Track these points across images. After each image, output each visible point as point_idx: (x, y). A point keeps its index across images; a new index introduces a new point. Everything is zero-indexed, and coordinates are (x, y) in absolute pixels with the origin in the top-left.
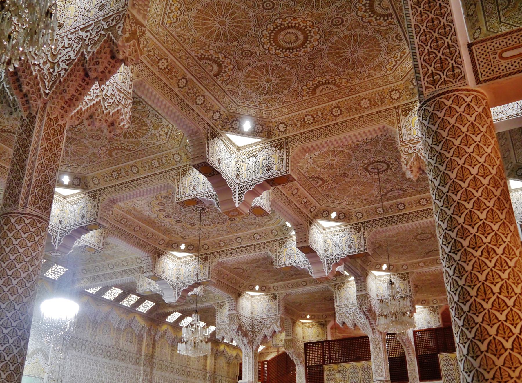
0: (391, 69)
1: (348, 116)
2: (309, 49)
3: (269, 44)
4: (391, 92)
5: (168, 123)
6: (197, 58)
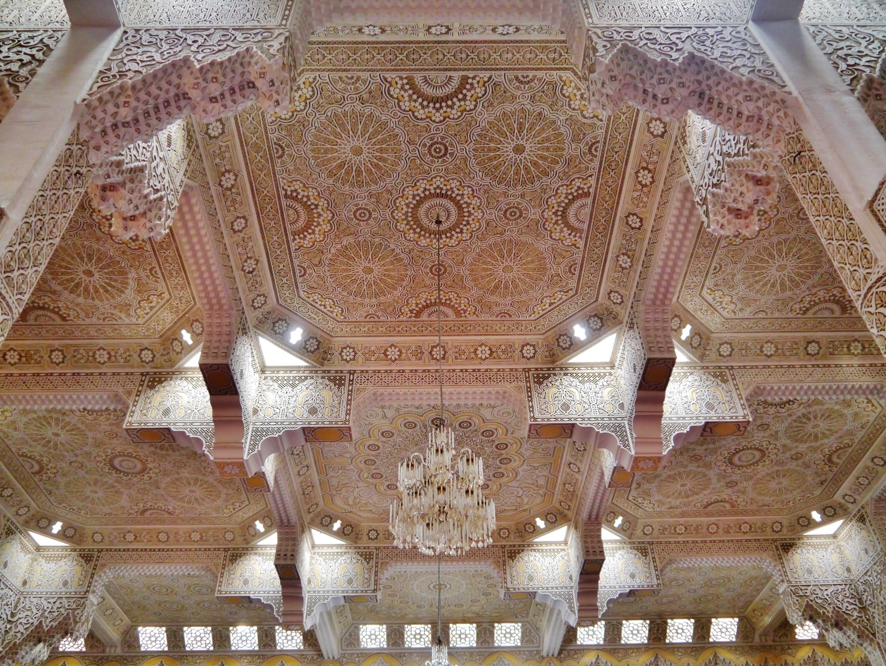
6: (284, 192)
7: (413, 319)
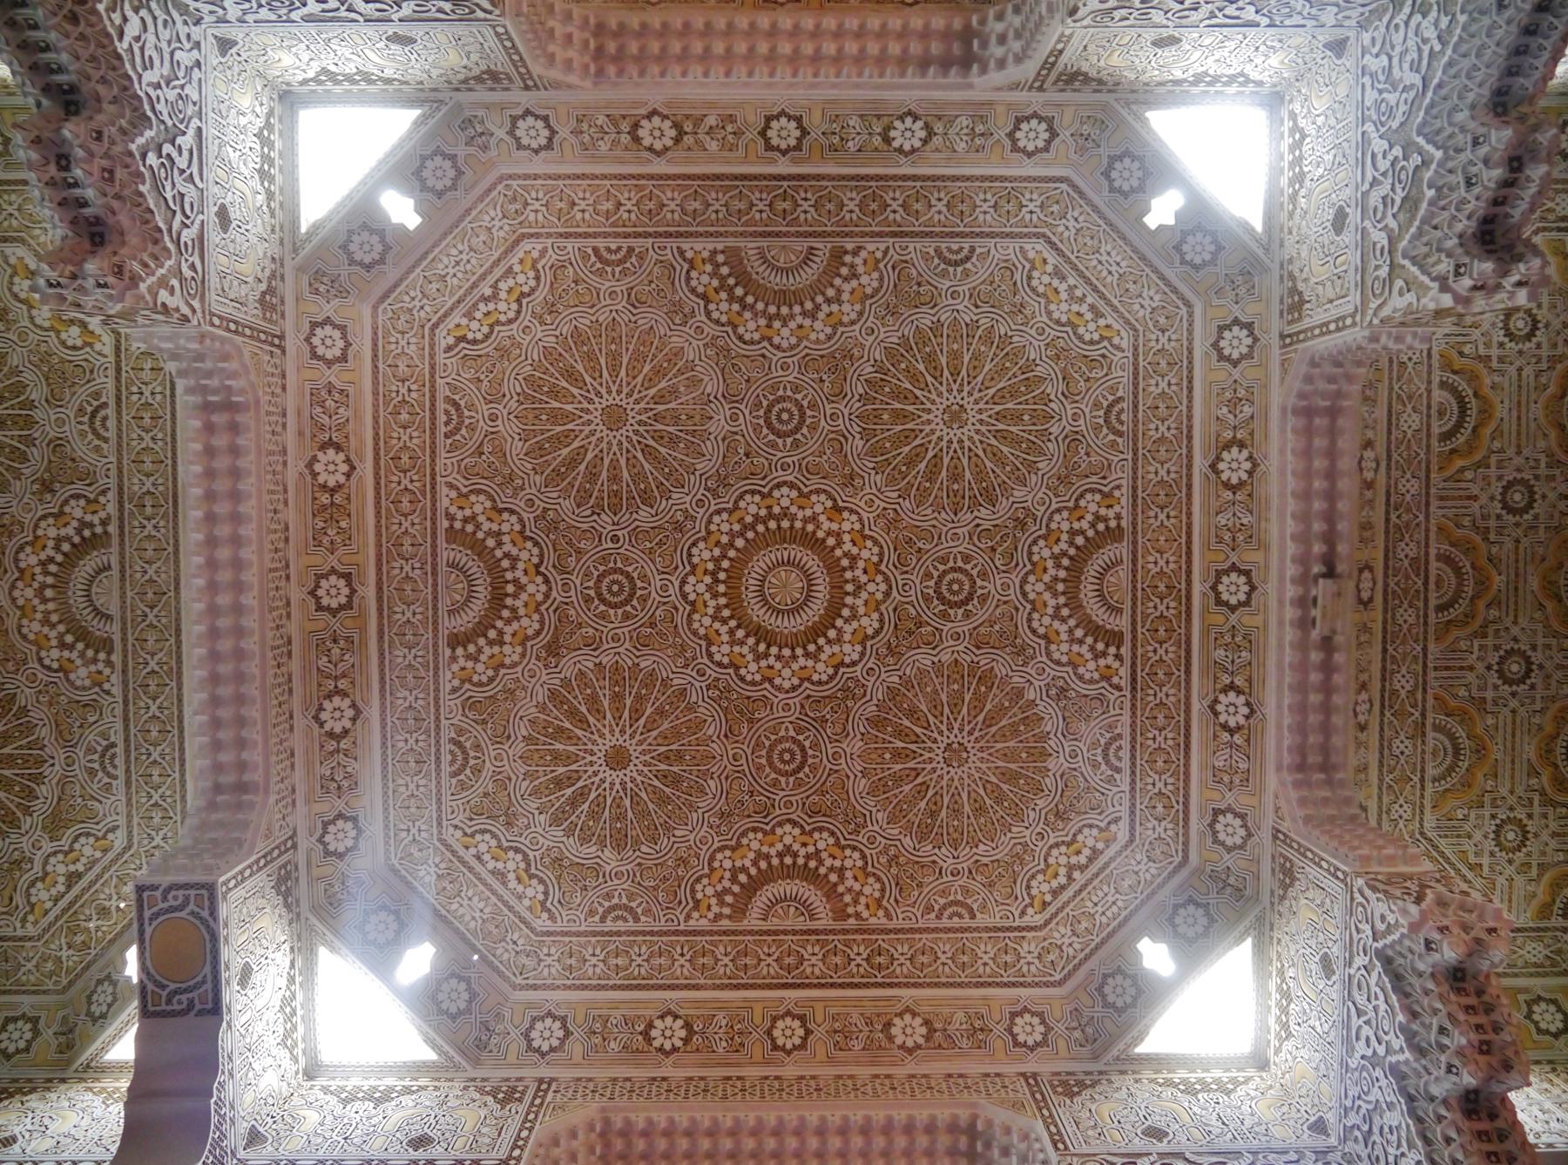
0: (1045, 904)
1: (830, 1060)
2: (822, 670)
3: (708, 579)
4: (1014, 1015)
5: (122, 821)
7: (725, 923)
